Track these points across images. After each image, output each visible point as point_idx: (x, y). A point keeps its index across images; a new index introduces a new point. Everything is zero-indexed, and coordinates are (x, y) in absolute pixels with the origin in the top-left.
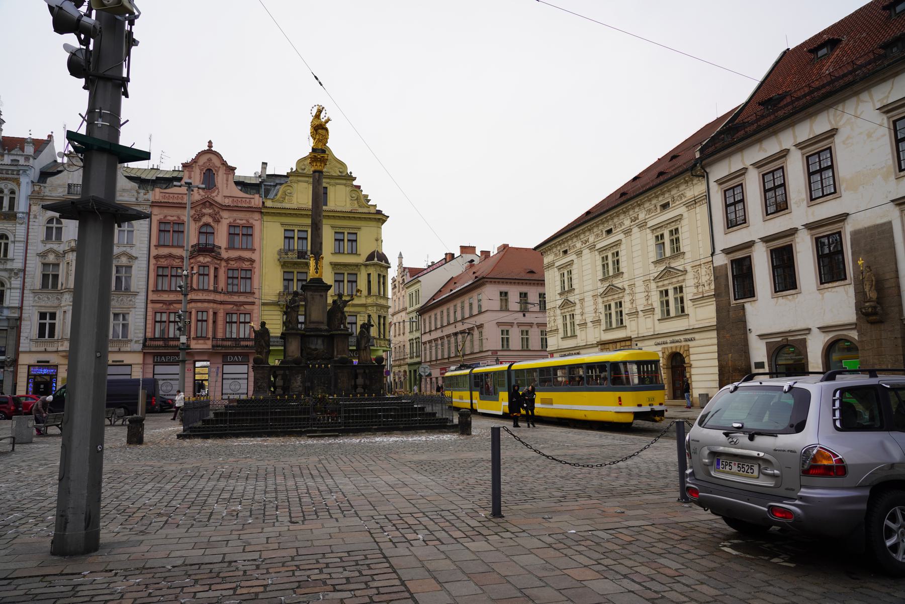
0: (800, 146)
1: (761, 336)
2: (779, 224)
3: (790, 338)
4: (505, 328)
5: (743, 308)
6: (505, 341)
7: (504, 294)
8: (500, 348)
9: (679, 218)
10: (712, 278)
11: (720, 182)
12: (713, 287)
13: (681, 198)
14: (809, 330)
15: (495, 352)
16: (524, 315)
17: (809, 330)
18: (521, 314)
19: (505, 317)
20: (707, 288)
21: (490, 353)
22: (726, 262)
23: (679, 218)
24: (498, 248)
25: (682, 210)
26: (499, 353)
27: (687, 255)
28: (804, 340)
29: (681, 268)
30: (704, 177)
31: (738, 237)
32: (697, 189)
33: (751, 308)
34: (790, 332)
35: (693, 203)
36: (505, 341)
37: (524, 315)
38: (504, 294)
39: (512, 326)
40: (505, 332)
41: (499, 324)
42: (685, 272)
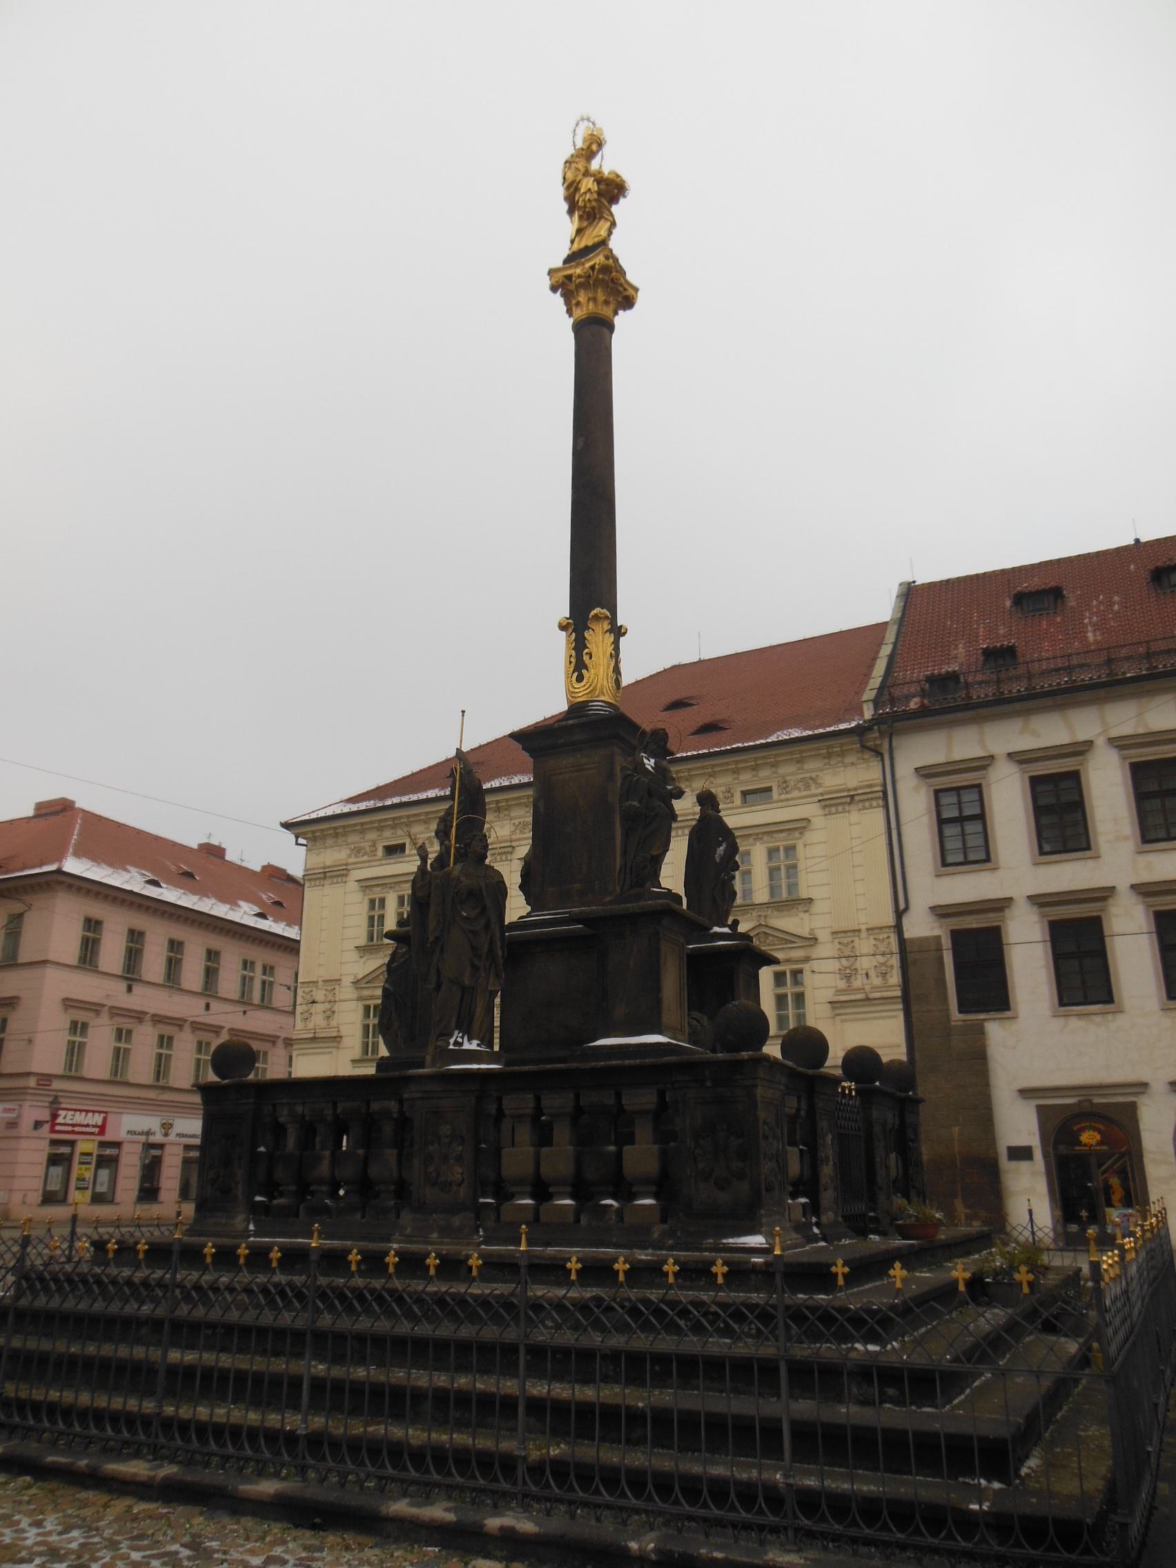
0: (1120, 744)
1: (1026, 1093)
2: (1069, 875)
3: (1097, 1100)
4: (82, 1016)
5: (980, 1031)
6: (75, 1052)
7: (93, 925)
8: (60, 1071)
9: (801, 826)
10: (895, 961)
11: (925, 773)
12: (895, 978)
13: (808, 787)
14: (1145, 1085)
15: (45, 1079)
16: (130, 989)
17: (1143, 1086)
18: (123, 986)
19: (87, 987)
20: (877, 981)
21: (32, 1082)
22: (937, 932)
23: (801, 826)
24: (39, 806)
25: (809, 810)
26: (57, 1085)
27: (818, 907)
28: (1132, 1109)
29: (805, 933)
30: (880, 754)
31: (968, 887)
32: (860, 773)
33: (996, 1032)
34: (1101, 1087)
35: (851, 799)
36: (75, 1052)
37: (130, 989)
38: (93, 925)
39: (97, 1013)
40: (78, 1028)
41: (69, 1004)
42: (813, 940)
